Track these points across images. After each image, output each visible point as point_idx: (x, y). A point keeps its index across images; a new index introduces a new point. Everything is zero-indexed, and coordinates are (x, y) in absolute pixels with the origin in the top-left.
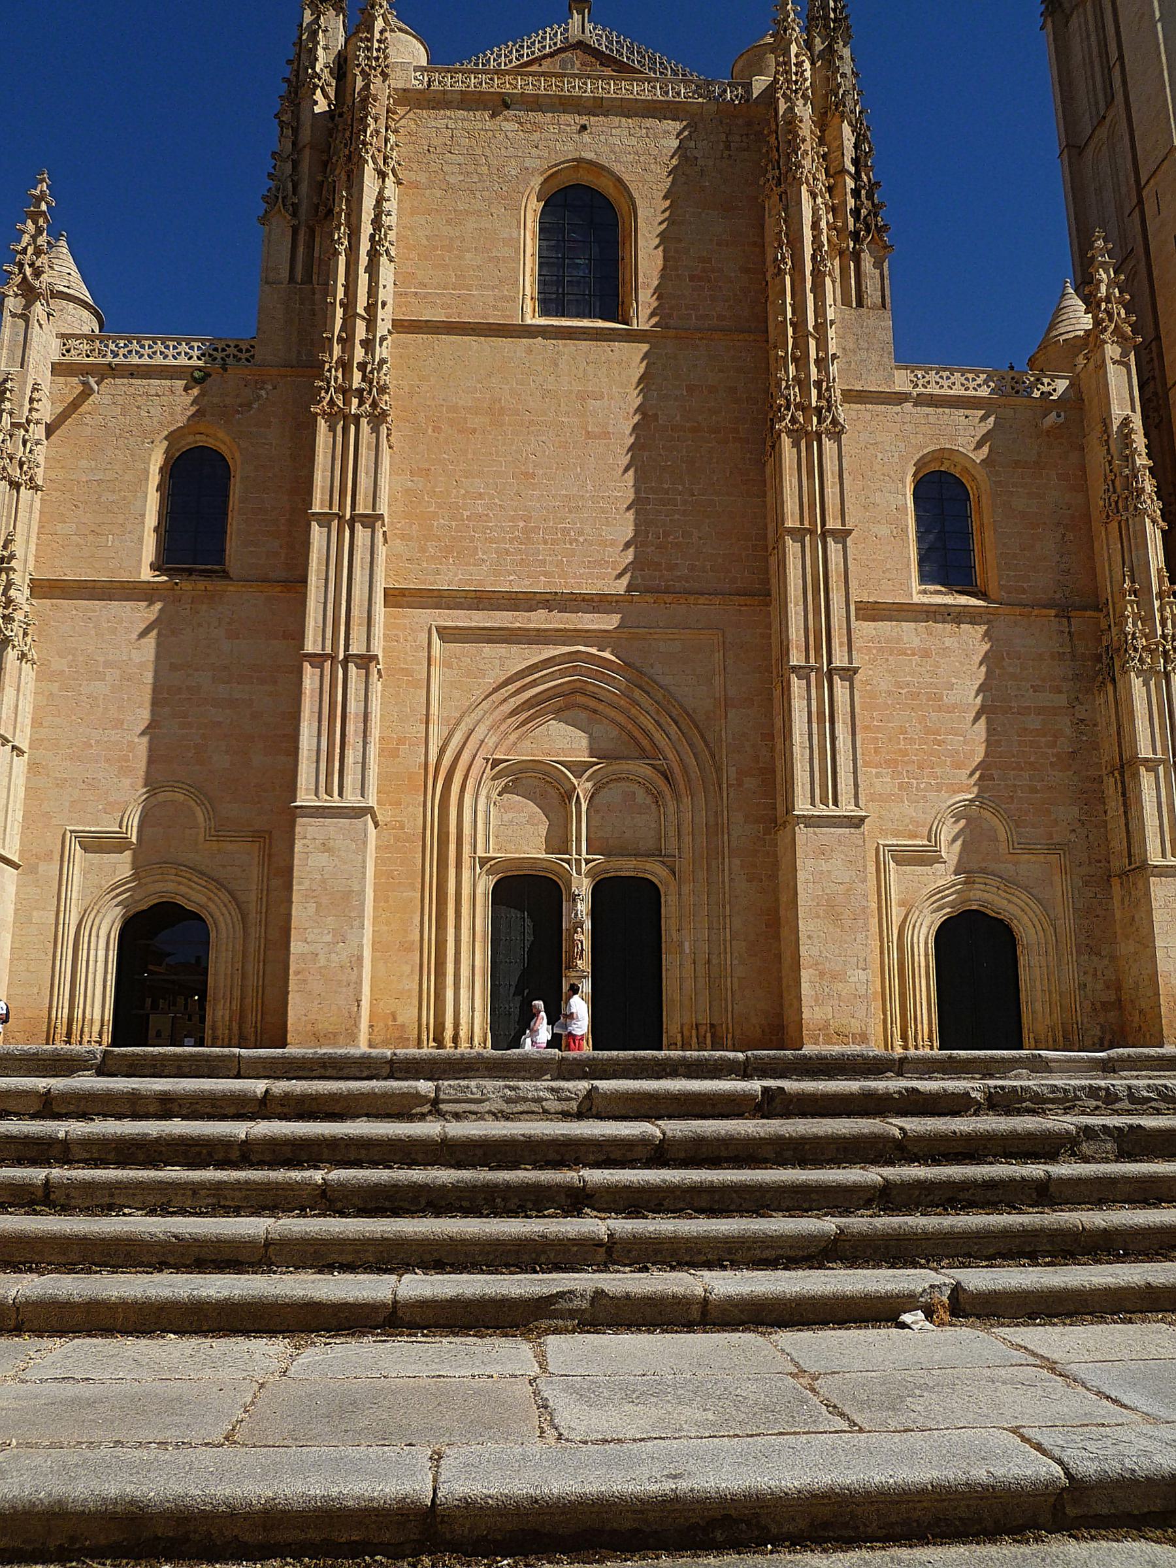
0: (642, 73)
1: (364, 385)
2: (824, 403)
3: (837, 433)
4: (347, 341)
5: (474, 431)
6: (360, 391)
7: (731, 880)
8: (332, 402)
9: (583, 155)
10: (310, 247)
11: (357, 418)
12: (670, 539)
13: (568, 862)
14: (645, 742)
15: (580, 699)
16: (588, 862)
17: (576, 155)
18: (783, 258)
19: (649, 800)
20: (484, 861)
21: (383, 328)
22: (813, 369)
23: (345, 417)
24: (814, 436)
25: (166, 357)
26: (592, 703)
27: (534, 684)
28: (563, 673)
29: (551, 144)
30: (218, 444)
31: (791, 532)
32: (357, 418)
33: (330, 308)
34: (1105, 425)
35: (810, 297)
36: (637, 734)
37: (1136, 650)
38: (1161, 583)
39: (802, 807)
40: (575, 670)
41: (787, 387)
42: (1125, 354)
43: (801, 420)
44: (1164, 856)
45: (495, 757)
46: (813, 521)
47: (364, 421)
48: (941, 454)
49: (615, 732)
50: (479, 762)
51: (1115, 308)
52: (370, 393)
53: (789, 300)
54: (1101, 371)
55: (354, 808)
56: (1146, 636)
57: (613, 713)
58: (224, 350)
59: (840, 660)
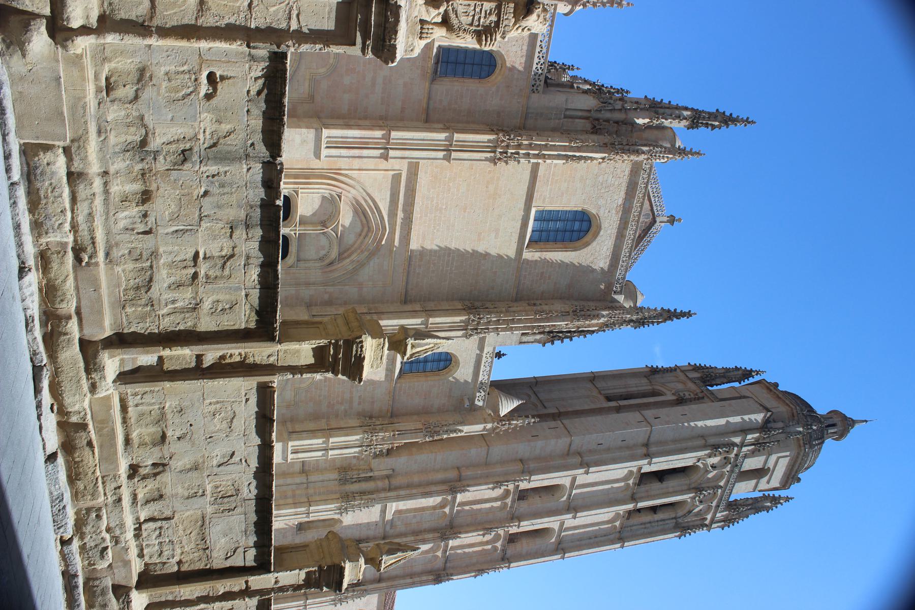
0: (635, 249)
1: (509, 155)
2: (479, 331)
3: (467, 336)
4: (530, 146)
5: (487, 187)
6: (506, 153)
7: (286, 290)
8: (503, 141)
9: (602, 230)
10: (580, 118)
11: (494, 152)
12: (432, 265)
13: (295, 226)
14: (346, 254)
15: (366, 229)
16: (295, 234)
17: (603, 227)
18: (577, 143)
19: (321, 255)
20: (297, 193)
21: (532, 161)
22: (524, 152)
23: (495, 147)
24: (493, 150)
25: (537, 64)
26: (364, 234)
27: (373, 213)
28: (377, 225)
29: (609, 218)
30: (496, 75)
31: (427, 321)
32: (494, 152)
33: (546, 138)
34: (461, 423)
35: (556, 153)
36: (350, 251)
37: (372, 436)
38: (397, 443)
39: (326, 132)
40: (378, 229)
41: (518, 140)
42: (487, 430)
43: (503, 145)
44: (292, 446)
45: (343, 197)
46: (430, 328)
47: (492, 154)
48: (457, 363)
49: (351, 242)
50: (340, 190)
51: (506, 427)
52: (505, 157)
53: (557, 144)
54: (483, 421)
55: (320, 153)
56: (377, 439)
57: (359, 242)
58: (539, 79)
59: (392, 153)
